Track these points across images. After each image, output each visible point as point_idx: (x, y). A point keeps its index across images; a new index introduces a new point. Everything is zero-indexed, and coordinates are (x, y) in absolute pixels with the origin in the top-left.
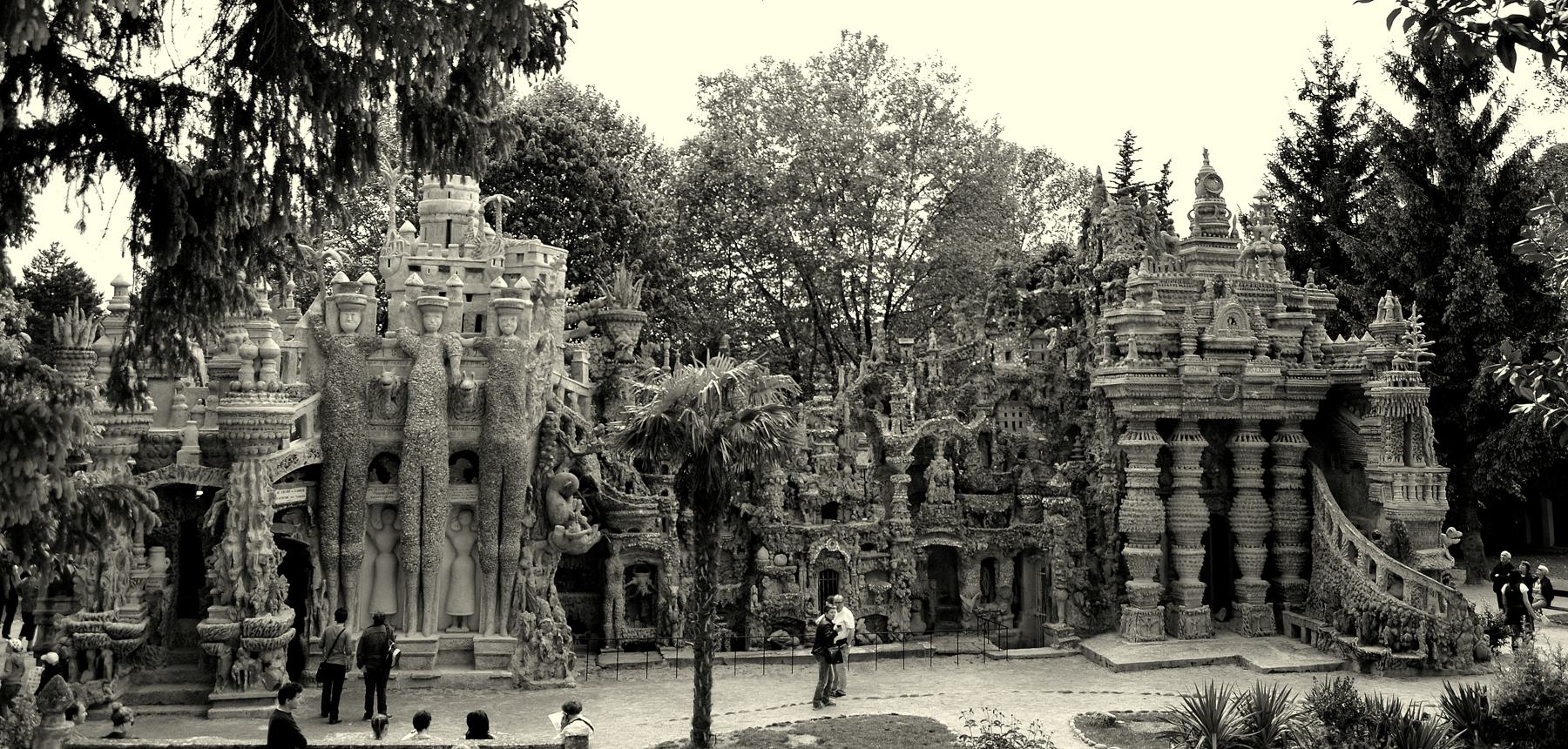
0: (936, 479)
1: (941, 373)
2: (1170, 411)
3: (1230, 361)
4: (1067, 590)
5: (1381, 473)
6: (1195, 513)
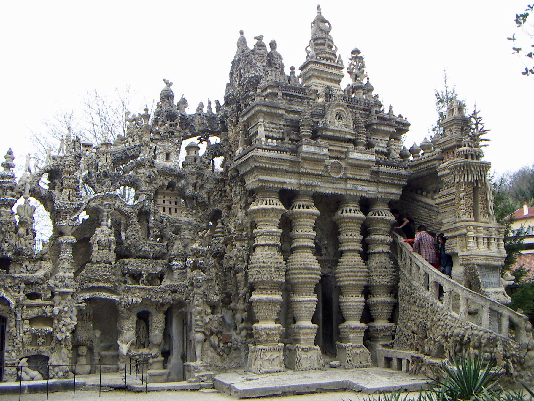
0: (98, 243)
1: (109, 161)
2: (291, 184)
3: (338, 147)
4: (203, 333)
5: (456, 229)
6: (309, 266)
